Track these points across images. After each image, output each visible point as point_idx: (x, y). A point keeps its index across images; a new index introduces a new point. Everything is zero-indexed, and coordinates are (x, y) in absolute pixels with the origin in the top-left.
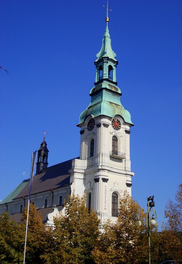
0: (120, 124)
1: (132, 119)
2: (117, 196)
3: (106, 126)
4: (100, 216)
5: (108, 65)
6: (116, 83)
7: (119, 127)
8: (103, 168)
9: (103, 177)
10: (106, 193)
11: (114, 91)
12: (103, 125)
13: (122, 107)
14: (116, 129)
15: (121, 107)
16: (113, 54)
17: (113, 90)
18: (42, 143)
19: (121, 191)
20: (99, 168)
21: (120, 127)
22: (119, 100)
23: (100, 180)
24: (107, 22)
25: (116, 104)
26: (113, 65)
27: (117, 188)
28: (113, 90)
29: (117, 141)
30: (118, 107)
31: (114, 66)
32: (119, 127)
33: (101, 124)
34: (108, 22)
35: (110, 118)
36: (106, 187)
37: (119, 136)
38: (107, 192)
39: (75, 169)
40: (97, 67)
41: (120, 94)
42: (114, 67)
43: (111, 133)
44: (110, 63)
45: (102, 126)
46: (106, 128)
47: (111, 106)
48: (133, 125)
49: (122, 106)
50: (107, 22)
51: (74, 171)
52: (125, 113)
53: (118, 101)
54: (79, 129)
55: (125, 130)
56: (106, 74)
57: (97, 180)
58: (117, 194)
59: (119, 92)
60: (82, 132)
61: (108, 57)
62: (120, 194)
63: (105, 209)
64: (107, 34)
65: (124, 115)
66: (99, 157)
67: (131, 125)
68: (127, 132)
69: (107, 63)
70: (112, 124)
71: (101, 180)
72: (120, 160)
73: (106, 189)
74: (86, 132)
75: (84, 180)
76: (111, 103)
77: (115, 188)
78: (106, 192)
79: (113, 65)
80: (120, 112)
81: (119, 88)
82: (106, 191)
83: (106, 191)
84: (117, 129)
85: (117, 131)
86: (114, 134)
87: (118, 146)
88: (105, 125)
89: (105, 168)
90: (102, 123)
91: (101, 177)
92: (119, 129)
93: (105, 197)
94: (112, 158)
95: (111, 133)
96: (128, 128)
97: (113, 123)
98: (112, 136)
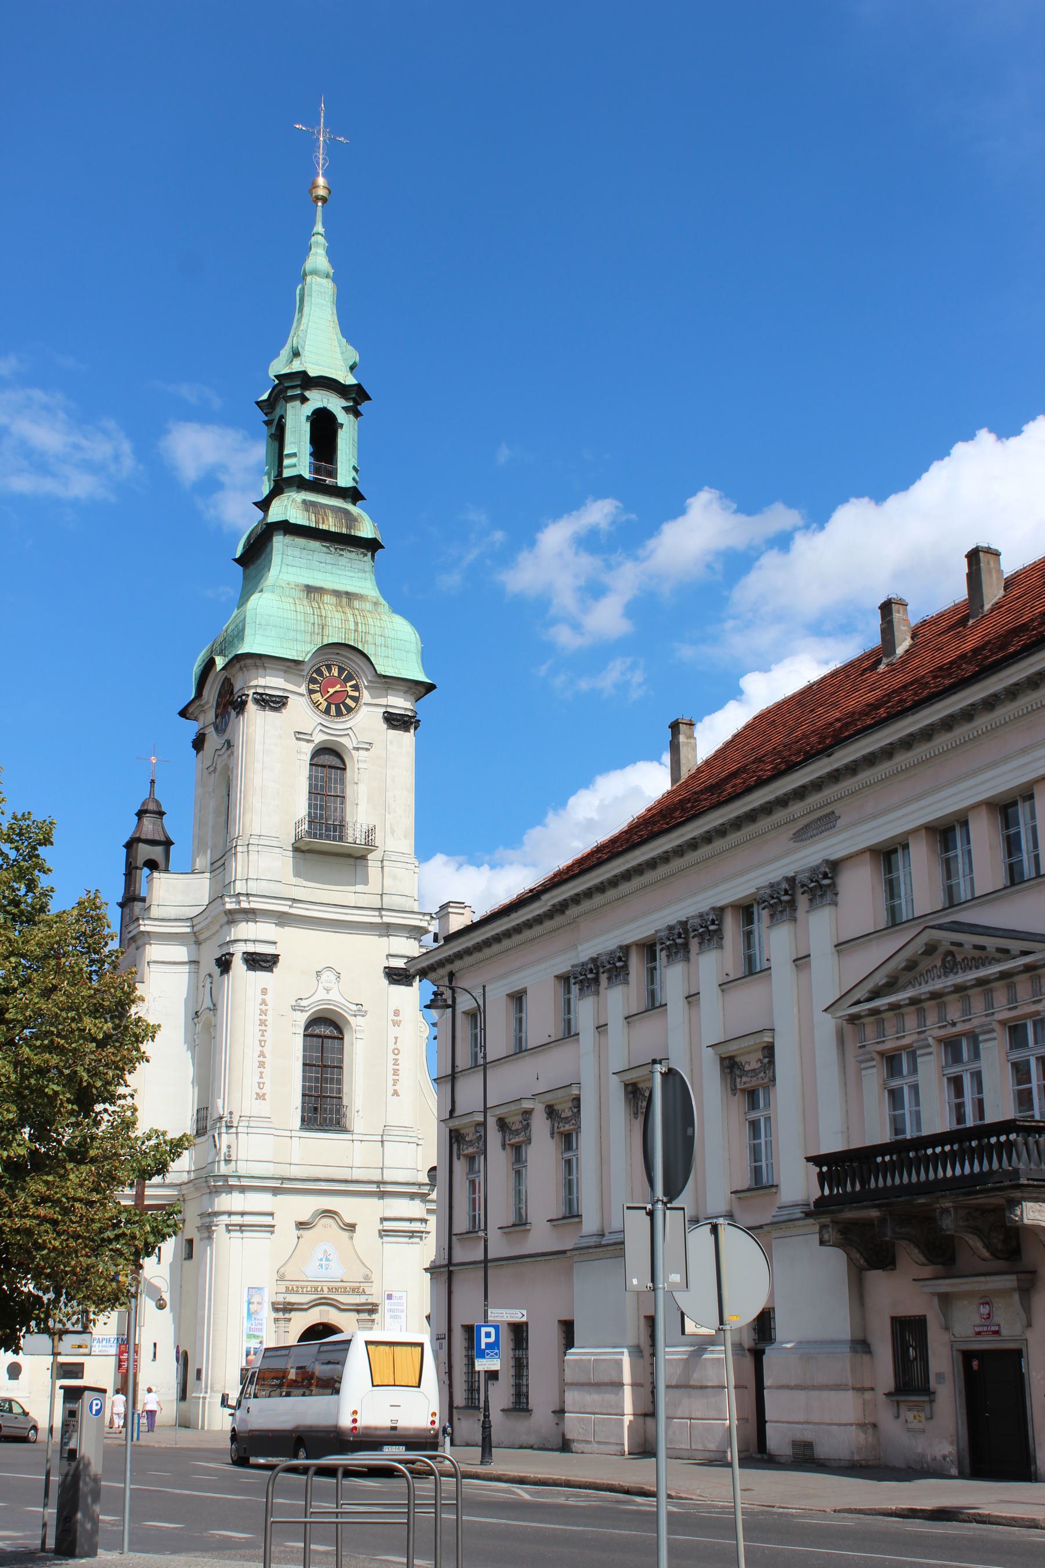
0: (356, 688)
1: (426, 660)
2: (341, 1032)
3: (273, 703)
4: (234, 1130)
5: (308, 409)
6: (353, 495)
7: (348, 701)
8: (245, 905)
9: (251, 948)
10: (263, 1023)
11: (333, 529)
12: (257, 701)
13: (376, 604)
14: (344, 712)
15: (368, 606)
16: (342, 353)
17: (330, 525)
18: (143, 804)
19: (354, 1008)
20: (228, 906)
21: (356, 699)
22: (364, 571)
23: (233, 965)
24: (320, 204)
25: (347, 593)
26: (335, 404)
27: (334, 996)
28: (325, 527)
29: (344, 769)
30: (356, 604)
31: (346, 409)
32: (348, 701)
33: (248, 695)
34: (324, 200)
35: (289, 666)
36: (264, 991)
37: (350, 747)
38: (270, 1018)
39: (146, 922)
40: (268, 423)
41: (371, 546)
42: (342, 417)
43: (300, 736)
44: (318, 399)
45: (251, 707)
46: (270, 715)
47: (300, 608)
48: (430, 688)
49: (382, 600)
50: (320, 204)
51: (142, 928)
52: (387, 633)
53: (360, 575)
54: (191, 729)
55: (384, 713)
56: (294, 455)
57: (224, 964)
58: (341, 1024)
59: (366, 530)
60: (199, 743)
61: (304, 373)
62: (351, 1019)
63: (261, 1097)
64: (318, 258)
65: (379, 640)
66: (235, 854)
67: (421, 689)
68: (395, 721)
69: (304, 400)
70: (311, 692)
71: (238, 964)
72: (352, 861)
73: (264, 1002)
74: (213, 740)
75: (193, 966)
76: (311, 590)
77: (321, 995)
78: (263, 1017)
79: (335, 404)
80: (352, 627)
81: (366, 517)
82: (263, 1012)
83: (263, 1012)
84: (339, 713)
85: (339, 725)
86: (319, 738)
87: (349, 792)
88: (263, 700)
89: (253, 905)
90: (251, 692)
91: (238, 950)
92: (350, 710)
93: (262, 1043)
94: (308, 855)
95: (299, 736)
96: (400, 703)
97: (316, 687)
98: (308, 749)
